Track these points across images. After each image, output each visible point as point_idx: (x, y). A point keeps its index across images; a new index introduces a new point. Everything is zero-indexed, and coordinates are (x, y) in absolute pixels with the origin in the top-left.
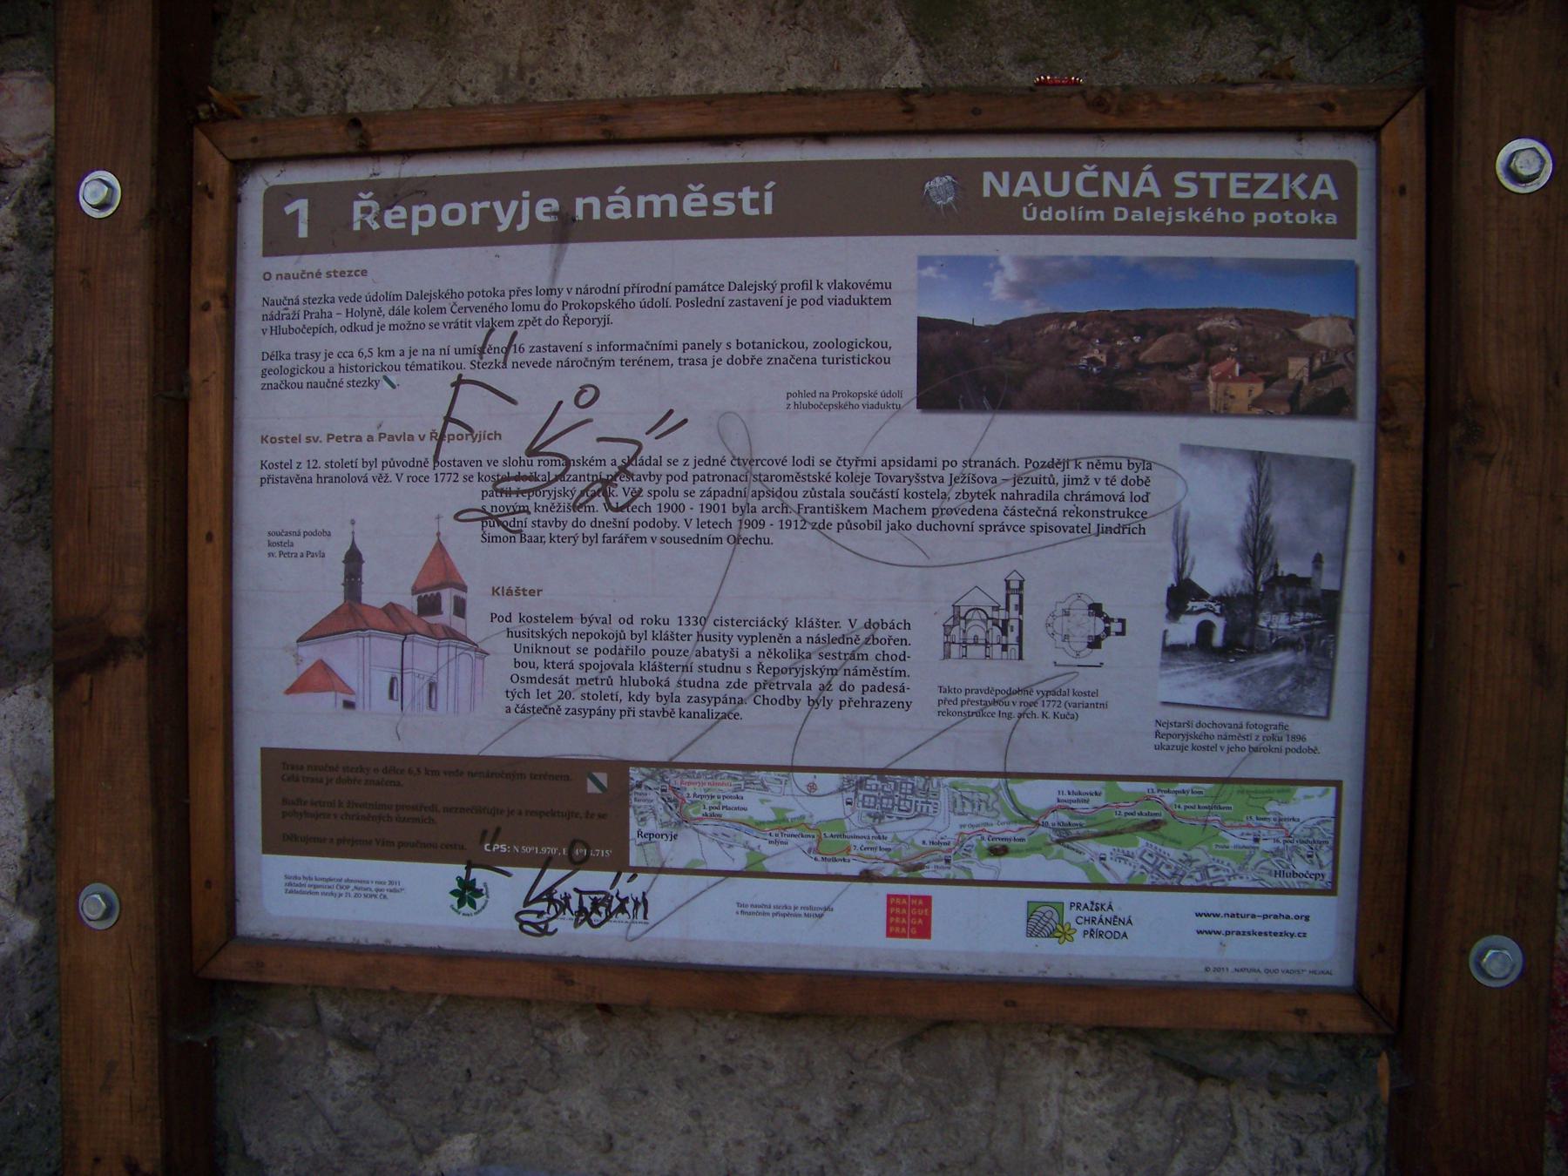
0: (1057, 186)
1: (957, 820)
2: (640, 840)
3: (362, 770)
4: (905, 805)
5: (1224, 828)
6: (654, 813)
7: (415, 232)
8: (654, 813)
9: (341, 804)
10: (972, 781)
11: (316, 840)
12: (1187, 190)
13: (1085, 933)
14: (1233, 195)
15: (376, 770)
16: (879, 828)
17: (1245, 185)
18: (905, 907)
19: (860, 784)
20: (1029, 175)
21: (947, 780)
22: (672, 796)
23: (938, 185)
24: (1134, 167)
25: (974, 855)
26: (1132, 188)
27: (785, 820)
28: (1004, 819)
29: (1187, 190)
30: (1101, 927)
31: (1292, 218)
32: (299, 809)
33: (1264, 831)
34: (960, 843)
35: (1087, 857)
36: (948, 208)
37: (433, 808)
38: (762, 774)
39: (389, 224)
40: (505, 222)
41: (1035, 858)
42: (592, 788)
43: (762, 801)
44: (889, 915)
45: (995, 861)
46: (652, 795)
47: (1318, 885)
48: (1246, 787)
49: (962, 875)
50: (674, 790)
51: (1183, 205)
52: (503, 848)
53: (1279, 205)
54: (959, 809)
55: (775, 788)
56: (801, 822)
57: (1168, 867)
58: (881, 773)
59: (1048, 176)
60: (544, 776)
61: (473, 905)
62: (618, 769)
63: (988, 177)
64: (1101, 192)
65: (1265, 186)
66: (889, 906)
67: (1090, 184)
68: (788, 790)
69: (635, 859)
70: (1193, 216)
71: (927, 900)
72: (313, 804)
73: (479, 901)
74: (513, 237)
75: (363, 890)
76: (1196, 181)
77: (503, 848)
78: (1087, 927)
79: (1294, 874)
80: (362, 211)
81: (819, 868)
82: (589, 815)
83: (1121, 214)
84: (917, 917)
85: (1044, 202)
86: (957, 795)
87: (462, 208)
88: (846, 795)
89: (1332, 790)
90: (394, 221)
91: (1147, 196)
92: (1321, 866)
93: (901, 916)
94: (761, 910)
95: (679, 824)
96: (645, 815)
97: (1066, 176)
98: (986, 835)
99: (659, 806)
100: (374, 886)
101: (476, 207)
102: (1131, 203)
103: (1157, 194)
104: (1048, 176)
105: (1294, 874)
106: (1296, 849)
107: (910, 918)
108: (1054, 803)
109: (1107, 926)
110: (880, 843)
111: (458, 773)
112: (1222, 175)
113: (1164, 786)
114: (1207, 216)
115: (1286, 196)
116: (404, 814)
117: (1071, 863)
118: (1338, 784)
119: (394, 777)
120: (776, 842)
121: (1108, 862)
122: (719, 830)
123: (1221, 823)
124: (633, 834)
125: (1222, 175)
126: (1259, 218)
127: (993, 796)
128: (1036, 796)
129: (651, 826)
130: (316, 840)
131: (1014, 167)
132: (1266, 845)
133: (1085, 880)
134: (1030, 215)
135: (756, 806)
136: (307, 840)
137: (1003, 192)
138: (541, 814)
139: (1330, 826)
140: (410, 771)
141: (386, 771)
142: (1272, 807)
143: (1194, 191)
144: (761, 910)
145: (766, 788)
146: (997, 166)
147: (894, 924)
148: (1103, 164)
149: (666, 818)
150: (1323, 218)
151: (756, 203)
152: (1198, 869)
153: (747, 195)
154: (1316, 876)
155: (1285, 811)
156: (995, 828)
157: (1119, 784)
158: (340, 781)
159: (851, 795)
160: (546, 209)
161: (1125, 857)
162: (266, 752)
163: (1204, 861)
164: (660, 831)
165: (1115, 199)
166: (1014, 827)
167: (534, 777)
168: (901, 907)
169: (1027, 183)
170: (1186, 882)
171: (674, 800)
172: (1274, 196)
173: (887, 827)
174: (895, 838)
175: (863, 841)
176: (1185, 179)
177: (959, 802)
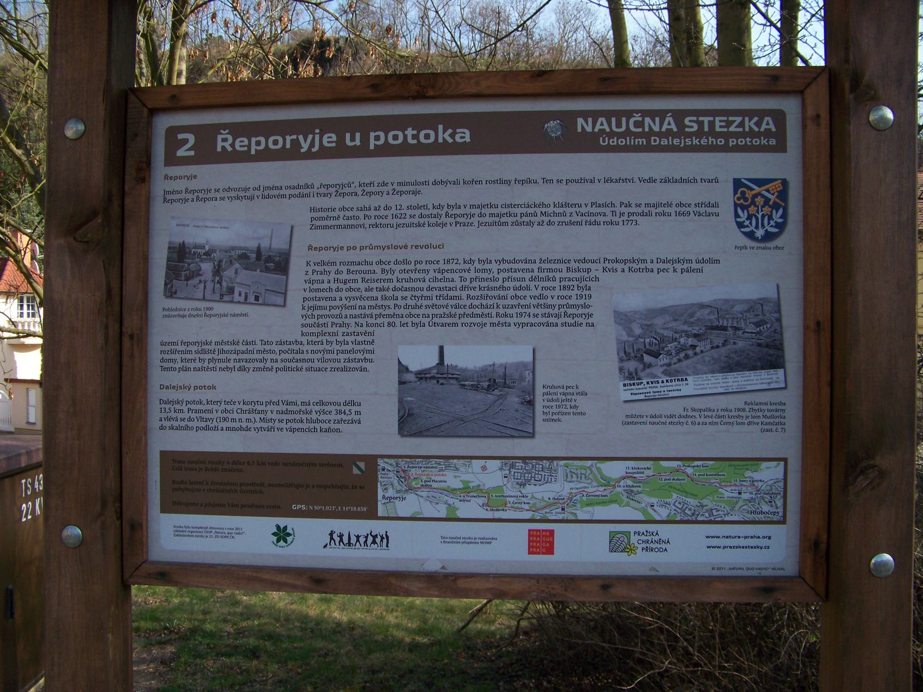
0: (619, 125)
3: (220, 463)
4: (538, 477)
6: (392, 485)
7: (253, 152)
8: (392, 485)
9: (207, 484)
11: (193, 504)
12: (692, 127)
13: (643, 549)
14: (718, 129)
16: (523, 491)
17: (724, 124)
18: (539, 536)
19: (513, 466)
20: (603, 120)
21: (562, 463)
23: (552, 125)
25: (578, 505)
26: (661, 126)
27: (469, 487)
28: (595, 484)
29: (692, 127)
30: (652, 545)
31: (751, 142)
32: (182, 486)
33: (744, 488)
34: (570, 499)
36: (557, 138)
37: (262, 485)
38: (455, 461)
39: (238, 148)
40: (305, 147)
43: (455, 477)
44: (529, 541)
45: (589, 509)
46: (391, 475)
47: (775, 518)
50: (404, 471)
52: (304, 507)
53: (744, 135)
54: (569, 479)
55: (463, 469)
56: (478, 488)
57: (690, 510)
58: (524, 459)
59: (613, 120)
62: (371, 460)
63: (580, 121)
64: (643, 127)
65: (735, 124)
66: (529, 536)
67: (637, 124)
68: (470, 470)
69: (381, 512)
70: (696, 141)
71: (552, 532)
72: (191, 483)
73: (289, 539)
74: (309, 156)
75: (221, 533)
76: (697, 122)
77: (304, 507)
78: (644, 545)
79: (762, 512)
80: (223, 142)
81: (489, 515)
82: (354, 487)
83: (655, 141)
84: (546, 542)
85: (612, 134)
87: (280, 139)
88: (504, 472)
89: (782, 463)
90: (241, 146)
91: (669, 131)
92: (777, 508)
93: (536, 542)
94: (455, 540)
95: (406, 491)
96: (386, 487)
97: (624, 119)
98: (585, 494)
99: (395, 481)
100: (226, 531)
101: (288, 138)
102: (660, 135)
103: (675, 130)
104: (613, 120)
105: (762, 512)
106: (763, 498)
107: (542, 543)
108: (623, 474)
109: (655, 545)
110: (524, 500)
112: (711, 119)
113: (687, 463)
114: (704, 141)
115: (747, 129)
116: (244, 488)
117: (635, 509)
118: (785, 460)
119: (240, 467)
120: (463, 501)
121: (655, 508)
124: (380, 497)
125: (711, 119)
126: (732, 142)
127: (589, 472)
128: (614, 470)
129: (391, 493)
130: (193, 504)
131: (595, 115)
132: (745, 496)
133: (643, 518)
134: (604, 141)
135: (452, 480)
136: (187, 505)
137: (589, 129)
138: (326, 487)
139: (781, 484)
141: (234, 463)
142: (748, 474)
143: (695, 127)
144: (455, 540)
145: (457, 469)
146: (585, 114)
147: (533, 547)
148: (645, 113)
149: (399, 488)
150: (768, 141)
151: (414, 137)
152: (707, 511)
154: (774, 513)
155: (756, 476)
156: (590, 490)
158: (207, 469)
159: (507, 472)
160: (330, 139)
161: (665, 505)
162: (163, 454)
163: (710, 506)
165: (651, 132)
166: (601, 489)
167: (321, 465)
168: (537, 536)
169: (602, 124)
170: (700, 518)
171: (403, 476)
172: (741, 130)
173: (529, 489)
174: (533, 496)
175: (514, 499)
176: (690, 121)
177: (569, 476)
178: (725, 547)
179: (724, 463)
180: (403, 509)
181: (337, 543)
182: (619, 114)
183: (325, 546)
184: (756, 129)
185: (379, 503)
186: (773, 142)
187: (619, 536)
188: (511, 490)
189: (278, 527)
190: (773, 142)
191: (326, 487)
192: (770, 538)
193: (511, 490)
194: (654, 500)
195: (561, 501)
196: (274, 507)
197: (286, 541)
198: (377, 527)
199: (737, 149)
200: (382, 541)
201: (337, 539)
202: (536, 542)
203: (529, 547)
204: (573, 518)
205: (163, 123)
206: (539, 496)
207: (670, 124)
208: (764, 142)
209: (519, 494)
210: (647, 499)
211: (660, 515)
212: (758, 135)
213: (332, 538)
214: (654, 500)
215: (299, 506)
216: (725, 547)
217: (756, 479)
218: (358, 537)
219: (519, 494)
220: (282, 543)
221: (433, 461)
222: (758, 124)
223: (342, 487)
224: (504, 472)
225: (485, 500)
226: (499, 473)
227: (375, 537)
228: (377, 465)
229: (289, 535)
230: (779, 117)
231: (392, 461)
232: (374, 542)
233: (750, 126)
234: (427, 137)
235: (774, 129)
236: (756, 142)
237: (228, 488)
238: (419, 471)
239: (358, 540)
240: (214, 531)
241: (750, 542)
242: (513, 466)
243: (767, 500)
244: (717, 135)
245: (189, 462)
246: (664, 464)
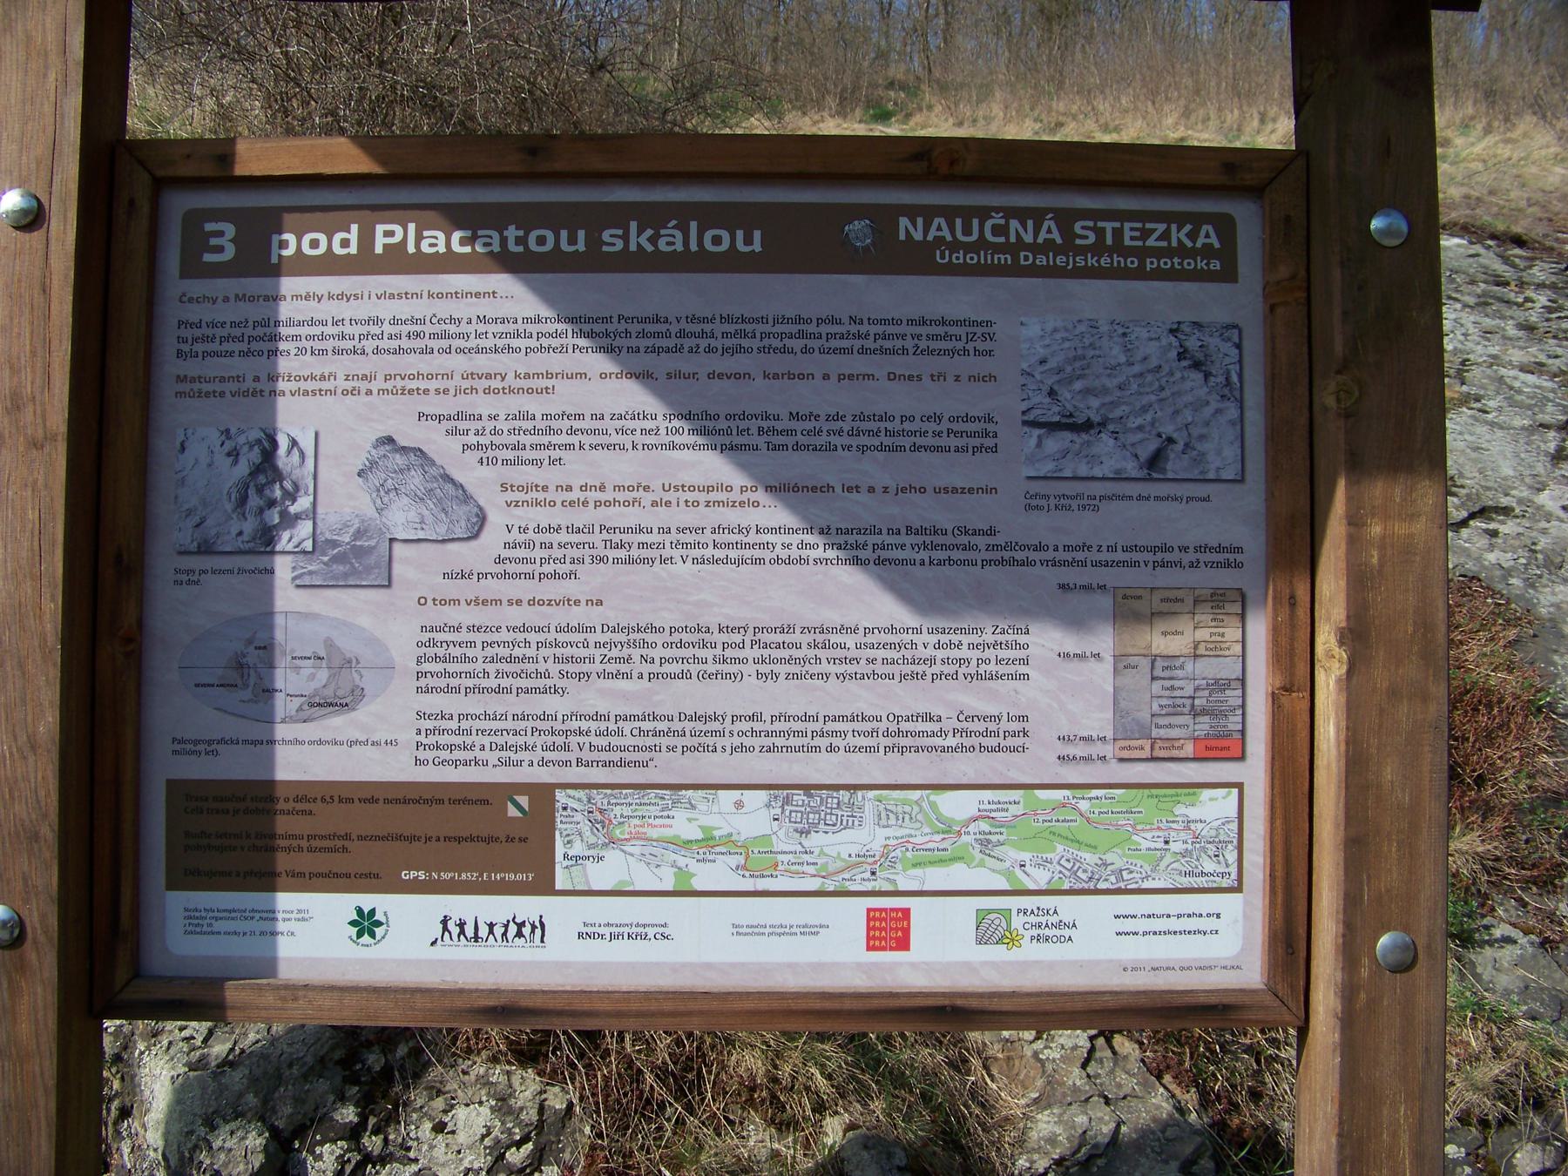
0: (967, 231)
1: (882, 833)
2: (566, 863)
4: (831, 819)
5: (1136, 832)
9: (248, 836)
10: (896, 794)
11: (223, 874)
14: (1127, 242)
16: (806, 843)
17: (1137, 234)
19: (787, 801)
20: (942, 221)
21: (871, 794)
22: (599, 817)
24: (1038, 215)
25: (899, 866)
26: (1036, 237)
27: (713, 838)
28: (927, 830)
34: (884, 855)
36: (866, 249)
37: (347, 837)
41: (958, 867)
42: (513, 812)
43: (689, 820)
45: (918, 871)
46: (578, 817)
47: (1225, 883)
48: (1154, 792)
50: (601, 811)
51: (1082, 251)
52: (422, 875)
53: (1169, 253)
54: (883, 822)
55: (702, 807)
56: (729, 839)
57: (1085, 871)
58: (807, 788)
59: (958, 222)
60: (465, 801)
61: (373, 935)
62: (543, 795)
63: (904, 222)
64: (1008, 238)
65: (1155, 235)
67: (996, 230)
68: (715, 809)
77: (422, 875)
81: (748, 885)
82: (510, 839)
83: (1026, 258)
85: (955, 246)
86: (881, 808)
88: (773, 812)
89: (1235, 791)
91: (1049, 243)
95: (605, 845)
96: (571, 839)
97: (975, 222)
98: (910, 846)
99: (586, 828)
102: (1035, 248)
103: (1059, 241)
104: (958, 222)
106: (1204, 850)
110: (806, 857)
111: (373, 800)
112: (1117, 225)
113: (1079, 793)
115: (1174, 244)
116: (314, 843)
118: (1239, 786)
121: (1027, 868)
122: (647, 850)
123: (1133, 827)
124: (559, 856)
125: (1117, 225)
127: (916, 809)
128: (958, 806)
129: (578, 848)
130: (223, 874)
131: (929, 213)
132: (1176, 847)
133: (1007, 887)
134: (943, 257)
135: (683, 825)
137: (918, 236)
139: (1234, 826)
141: (297, 799)
142: (1180, 810)
143: (1092, 238)
145: (693, 807)
146: (912, 212)
148: (1010, 213)
149: (592, 840)
153: (512, 233)
154: (1223, 875)
155: (1193, 813)
157: (1037, 792)
158: (247, 811)
159: (779, 811)
162: (172, 785)
163: (1119, 864)
166: (938, 837)
169: (939, 228)
170: (1102, 885)
171: (600, 821)
172: (1165, 244)
173: (815, 840)
176: (1083, 228)
178: (1145, 934)
179: (1134, 791)
180: (601, 875)
182: (967, 213)
184: (1189, 244)
186: (1216, 265)
190: (1216, 265)
191: (459, 840)
192: (1218, 916)
193: (784, 841)
194: (1026, 856)
195: (870, 860)
196: (369, 875)
204: (891, 888)
205: (180, 203)
206: (832, 851)
207: (1050, 231)
208: (1201, 264)
209: (799, 848)
210: (1013, 854)
211: (1035, 881)
212: (1192, 253)
214: (1026, 856)
215: (413, 874)
216: (1145, 934)
217: (1192, 817)
219: (799, 848)
221: (652, 793)
222: (1193, 236)
223: (490, 840)
224: (773, 812)
226: (764, 811)
228: (553, 800)
230: (1225, 226)
231: (581, 794)
234: (541, 241)
235: (1217, 245)
236: (1189, 265)
238: (627, 811)
242: (787, 801)
243: (1211, 853)
245: (215, 799)
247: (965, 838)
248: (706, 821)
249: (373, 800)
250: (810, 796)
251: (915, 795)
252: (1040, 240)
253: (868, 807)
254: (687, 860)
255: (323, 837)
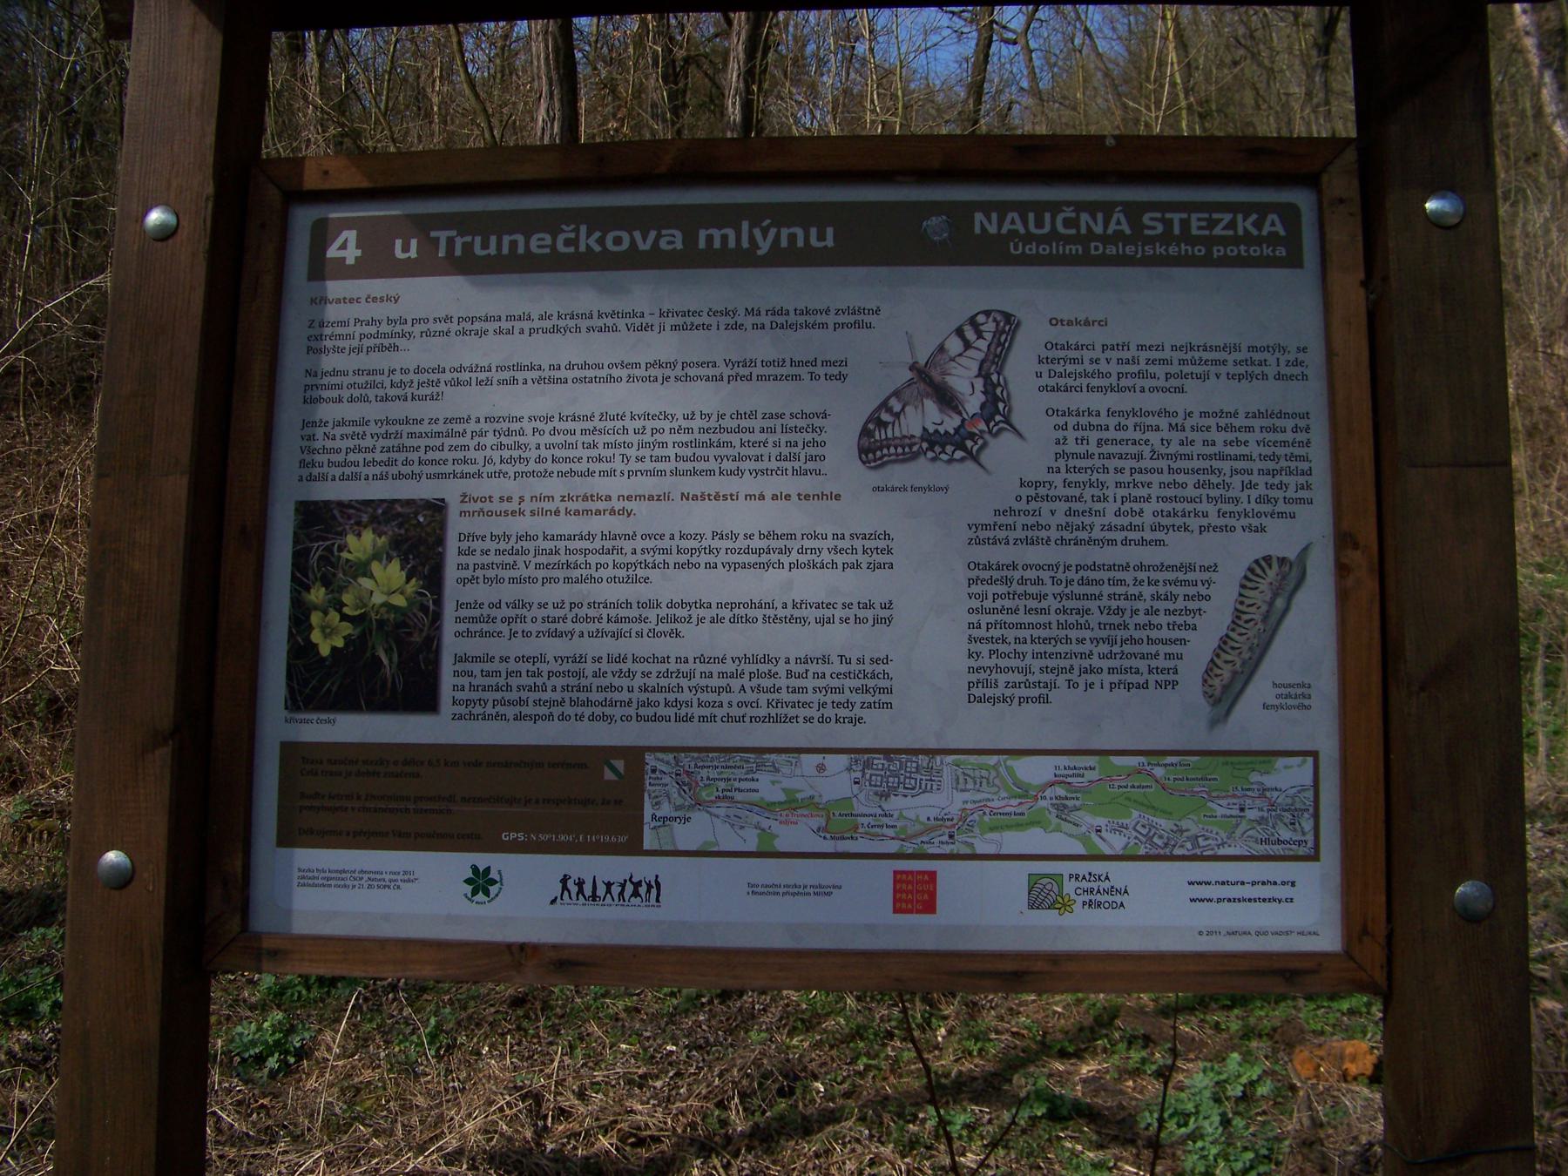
0: (1039, 225)
1: (959, 797)
4: (910, 783)
9: (359, 798)
10: (972, 759)
14: (1194, 232)
15: (395, 763)
16: (885, 806)
19: (868, 765)
20: (1015, 215)
21: (950, 759)
24: (1107, 208)
25: (977, 830)
28: (1004, 794)
29: (1154, 228)
34: (963, 819)
35: (1084, 829)
37: (451, 799)
38: (773, 756)
42: (609, 775)
44: (895, 891)
46: (667, 779)
49: (965, 850)
50: (688, 773)
51: (1151, 240)
53: (1236, 240)
54: (961, 786)
55: (785, 770)
56: (811, 803)
58: (887, 753)
59: (1031, 216)
62: (634, 756)
63: (979, 217)
64: (1078, 227)
67: (1067, 223)
68: (798, 772)
69: (649, 842)
70: (1160, 250)
71: (932, 875)
73: (493, 889)
75: (377, 881)
81: (828, 846)
83: (1096, 248)
85: (1029, 238)
88: (854, 775)
91: (1119, 235)
93: (907, 892)
94: (771, 890)
95: (691, 807)
97: (1047, 216)
98: (987, 810)
99: (674, 790)
102: (1105, 239)
103: (1128, 231)
104: (1031, 216)
107: (916, 894)
108: (1052, 778)
110: (885, 820)
112: (1184, 216)
113: (1154, 760)
114: (1173, 250)
115: (1240, 232)
120: (786, 822)
121: (1104, 834)
122: (732, 812)
124: (647, 817)
125: (1184, 216)
126: (1217, 251)
127: (993, 773)
128: (1035, 771)
129: (666, 810)
131: (1003, 208)
133: (1081, 850)
134: (1016, 248)
135: (767, 787)
137: (992, 230)
140: (430, 763)
143: (1160, 228)
144: (771, 890)
145: (777, 770)
146: (986, 207)
147: (900, 900)
148: (1080, 207)
149: (679, 801)
159: (859, 774)
164: (674, 814)
166: (1015, 802)
168: (908, 882)
169: (1013, 222)
171: (686, 782)
172: (1231, 233)
173: (895, 803)
176: (1152, 219)
179: (1208, 760)
180: (686, 836)
181: (574, 896)
182: (1040, 208)
183: (553, 902)
184: (1255, 232)
185: (646, 827)
186: (1281, 252)
187: (1045, 881)
188: (865, 804)
189: (475, 869)
190: (1281, 252)
194: (1101, 821)
197: (487, 893)
198: (641, 867)
199: (1224, 262)
200: (649, 891)
201: (574, 889)
202: (907, 892)
203: (895, 901)
206: (911, 814)
207: (1120, 223)
208: (1267, 251)
210: (1089, 820)
212: (1259, 241)
213: (565, 888)
214: (1101, 821)
215: (513, 835)
218: (609, 885)
220: (480, 896)
221: (738, 756)
222: (1258, 225)
224: (854, 775)
225: (822, 821)
226: (845, 775)
227: (637, 885)
229: (493, 882)
230: (1290, 215)
232: (636, 894)
233: (1245, 229)
236: (1255, 251)
237: (393, 805)
238: (713, 774)
239: (609, 891)
240: (366, 876)
241: (1247, 892)
242: (868, 765)
244: (1194, 241)
246: (1115, 760)
247: (1042, 803)
248: (787, 783)
249: (477, 764)
250: (890, 760)
251: (993, 760)
252: (1110, 231)
253: (946, 772)
254: (771, 822)
255: (430, 799)
